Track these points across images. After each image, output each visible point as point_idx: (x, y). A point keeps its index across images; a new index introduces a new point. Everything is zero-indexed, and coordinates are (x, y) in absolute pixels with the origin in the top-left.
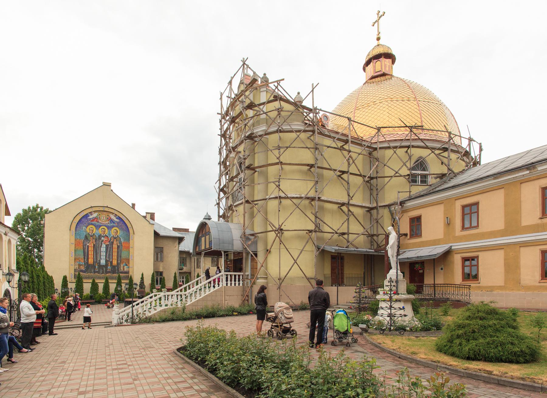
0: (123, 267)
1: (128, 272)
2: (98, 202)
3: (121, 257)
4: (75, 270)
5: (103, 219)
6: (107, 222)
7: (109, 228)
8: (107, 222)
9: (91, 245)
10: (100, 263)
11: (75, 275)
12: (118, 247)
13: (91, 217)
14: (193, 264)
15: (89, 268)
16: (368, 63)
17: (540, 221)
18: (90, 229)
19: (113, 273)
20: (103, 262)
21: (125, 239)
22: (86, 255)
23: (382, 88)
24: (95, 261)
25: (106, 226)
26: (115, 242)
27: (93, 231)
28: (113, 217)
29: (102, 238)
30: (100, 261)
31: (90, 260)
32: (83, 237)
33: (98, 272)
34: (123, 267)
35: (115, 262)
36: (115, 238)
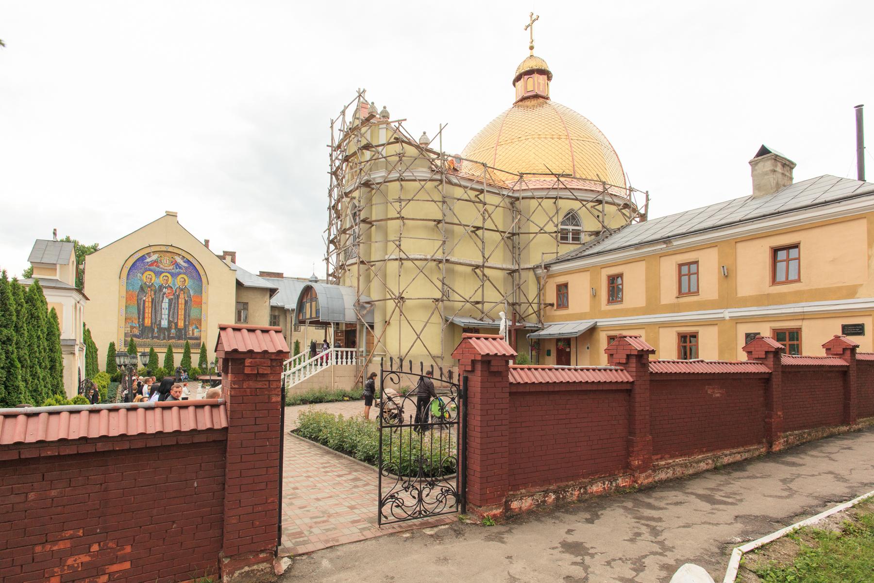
0: (193, 330)
1: (198, 338)
3: (189, 316)
4: (126, 335)
5: (166, 263)
6: (171, 267)
7: (174, 275)
8: (171, 267)
9: (148, 299)
10: (160, 324)
11: (125, 341)
12: (186, 302)
13: (149, 260)
14: (289, 325)
15: (145, 331)
16: (518, 79)
17: (676, 301)
18: (148, 277)
19: (179, 339)
20: (164, 324)
21: (195, 292)
22: (141, 313)
23: (534, 115)
24: (154, 321)
26: (182, 296)
28: (179, 260)
29: (164, 290)
31: (146, 320)
32: (137, 287)
33: (158, 338)
34: (193, 330)
35: (181, 324)
36: (182, 290)
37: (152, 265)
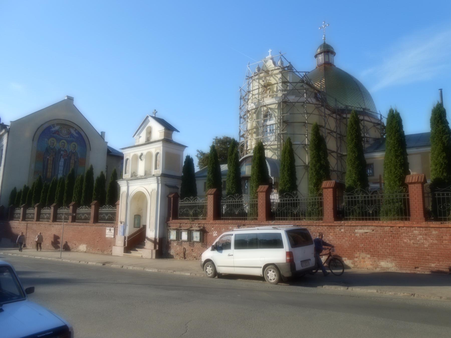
2: (63, 115)
6: (67, 136)
8: (67, 136)
12: (75, 162)
25: (65, 140)
27: (54, 143)
28: (73, 131)
31: (48, 174)
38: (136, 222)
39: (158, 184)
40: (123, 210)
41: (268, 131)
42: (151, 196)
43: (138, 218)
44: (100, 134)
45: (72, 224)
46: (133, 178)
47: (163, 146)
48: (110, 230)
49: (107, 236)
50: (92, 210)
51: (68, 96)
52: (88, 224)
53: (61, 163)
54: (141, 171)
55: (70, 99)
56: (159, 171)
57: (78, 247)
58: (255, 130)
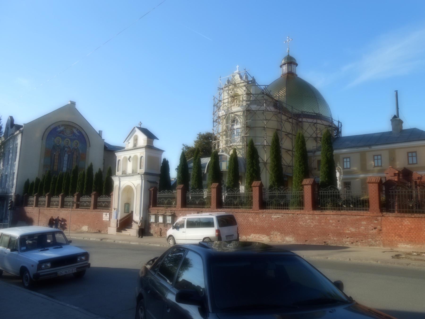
2: (66, 117)
6: (70, 135)
7: (72, 140)
8: (70, 135)
27: (59, 142)
30: (62, 168)
37: (60, 133)
38: (126, 208)
39: (142, 180)
40: (117, 200)
41: (235, 134)
42: (136, 189)
43: (128, 206)
44: (98, 132)
45: (77, 209)
46: (124, 175)
47: (146, 151)
48: (106, 215)
49: (104, 219)
50: (92, 199)
51: (71, 101)
52: (89, 210)
53: (66, 158)
54: (129, 170)
55: (73, 104)
56: (143, 171)
57: (81, 227)
58: (224, 133)
